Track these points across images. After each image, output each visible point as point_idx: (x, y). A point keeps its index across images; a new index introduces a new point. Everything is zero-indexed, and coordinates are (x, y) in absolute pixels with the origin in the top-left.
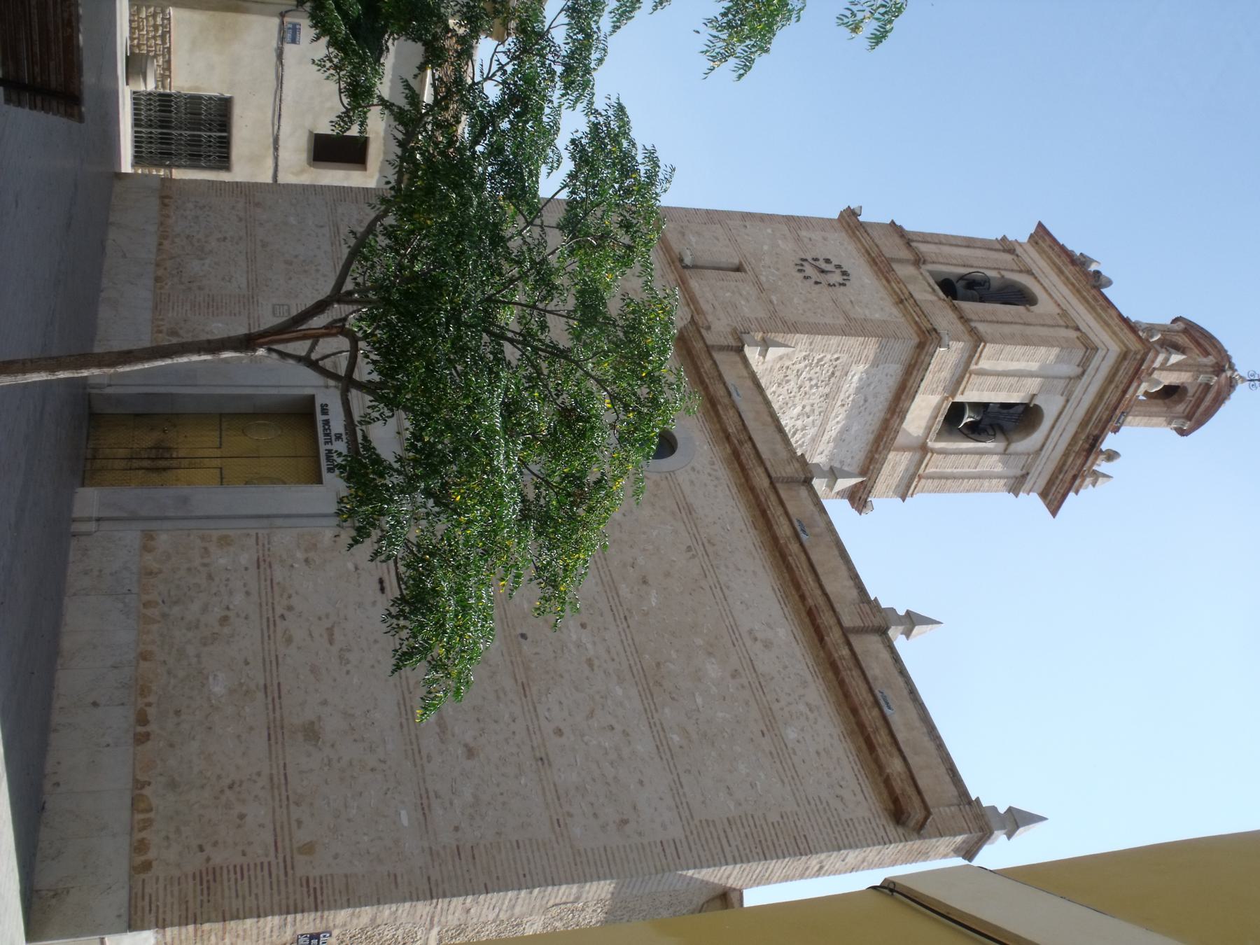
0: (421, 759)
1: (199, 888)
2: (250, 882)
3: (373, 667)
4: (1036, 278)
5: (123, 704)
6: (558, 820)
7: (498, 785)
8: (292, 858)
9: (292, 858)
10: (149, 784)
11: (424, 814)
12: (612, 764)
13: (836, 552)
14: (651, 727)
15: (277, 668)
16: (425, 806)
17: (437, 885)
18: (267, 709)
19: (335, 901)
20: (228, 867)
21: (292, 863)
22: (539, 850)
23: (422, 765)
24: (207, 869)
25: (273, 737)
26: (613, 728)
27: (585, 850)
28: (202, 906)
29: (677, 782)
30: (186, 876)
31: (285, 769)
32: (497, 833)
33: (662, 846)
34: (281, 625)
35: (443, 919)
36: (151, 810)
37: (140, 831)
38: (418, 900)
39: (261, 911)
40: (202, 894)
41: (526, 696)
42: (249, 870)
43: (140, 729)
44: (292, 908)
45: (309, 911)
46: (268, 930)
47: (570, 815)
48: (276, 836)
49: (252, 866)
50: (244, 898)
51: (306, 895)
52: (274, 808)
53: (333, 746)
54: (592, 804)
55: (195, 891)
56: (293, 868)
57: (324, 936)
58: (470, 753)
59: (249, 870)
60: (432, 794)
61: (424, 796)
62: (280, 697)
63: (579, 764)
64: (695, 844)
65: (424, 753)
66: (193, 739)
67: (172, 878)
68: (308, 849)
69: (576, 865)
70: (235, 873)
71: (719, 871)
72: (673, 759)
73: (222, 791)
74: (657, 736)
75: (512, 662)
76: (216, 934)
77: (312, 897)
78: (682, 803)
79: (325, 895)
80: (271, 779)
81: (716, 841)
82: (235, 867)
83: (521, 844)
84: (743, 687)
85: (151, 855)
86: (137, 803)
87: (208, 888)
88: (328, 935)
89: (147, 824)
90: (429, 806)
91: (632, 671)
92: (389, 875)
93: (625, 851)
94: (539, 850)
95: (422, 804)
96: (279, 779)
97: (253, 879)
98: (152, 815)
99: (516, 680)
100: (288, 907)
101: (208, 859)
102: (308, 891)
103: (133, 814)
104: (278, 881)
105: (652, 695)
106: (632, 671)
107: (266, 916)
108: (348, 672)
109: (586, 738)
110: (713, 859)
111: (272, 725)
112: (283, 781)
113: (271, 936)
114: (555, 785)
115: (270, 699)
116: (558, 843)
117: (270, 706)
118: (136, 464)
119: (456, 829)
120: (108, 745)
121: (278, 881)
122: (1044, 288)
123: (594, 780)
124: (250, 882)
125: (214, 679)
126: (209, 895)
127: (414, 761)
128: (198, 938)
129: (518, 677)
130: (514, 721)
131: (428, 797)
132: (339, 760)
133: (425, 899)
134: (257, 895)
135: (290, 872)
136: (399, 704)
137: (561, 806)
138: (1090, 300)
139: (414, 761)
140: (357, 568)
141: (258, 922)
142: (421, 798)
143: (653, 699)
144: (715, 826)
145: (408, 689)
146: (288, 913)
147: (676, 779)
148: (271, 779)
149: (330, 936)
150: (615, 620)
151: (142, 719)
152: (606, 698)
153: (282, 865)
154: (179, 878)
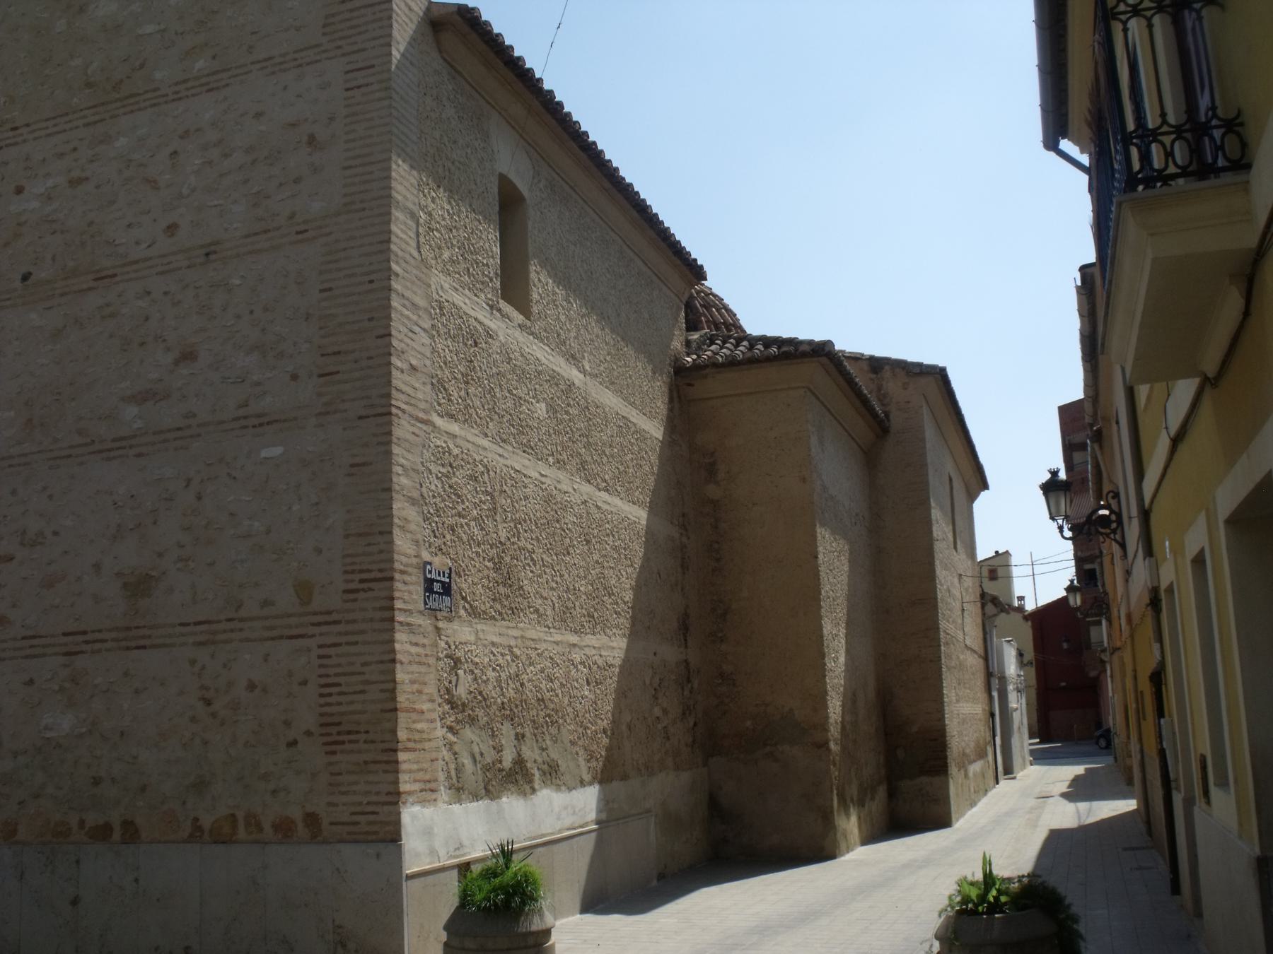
0: (189, 427)
1: (347, 746)
2: (344, 674)
3: (50, 497)
5: (78, 862)
6: (298, 233)
7: (239, 317)
8: (315, 614)
9: (315, 614)
10: (196, 820)
11: (268, 423)
12: (226, 156)
14: (180, 99)
15: (41, 637)
16: (256, 421)
17: (372, 406)
18: (99, 651)
19: (381, 552)
20: (321, 706)
21: (321, 613)
22: (336, 261)
23: (199, 426)
24: (322, 735)
25: (142, 642)
26: (175, 152)
27: (345, 195)
28: (373, 742)
29: (264, 64)
30: (330, 764)
31: (188, 624)
32: (307, 319)
33: (352, 89)
35: (422, 405)
36: (233, 815)
37: (261, 830)
38: (390, 433)
39: (386, 657)
40: (357, 742)
41: (115, 275)
42: (328, 676)
43: (117, 835)
44: (387, 614)
45: (392, 589)
46: (414, 650)
47: (292, 217)
48: (281, 637)
49: (323, 671)
50: (367, 682)
51: (370, 594)
52: (241, 641)
54: (281, 185)
55: (352, 751)
56: (329, 613)
57: (430, 572)
58: (188, 356)
59: (328, 676)
60: (241, 412)
61: (243, 422)
62: (85, 633)
63: (221, 202)
64: (356, 43)
66: (135, 758)
67: (330, 784)
68: (304, 591)
69: (364, 209)
70: (330, 695)
71: (397, 15)
72: (229, 70)
73: (214, 715)
74: (193, 91)
75: (62, 295)
76: (414, 722)
77: (371, 585)
78: (296, 59)
79: (370, 567)
80: (201, 644)
81: (355, 14)
82: (322, 695)
83: (326, 285)
85: (296, 813)
86: (222, 836)
87: (349, 733)
88: (428, 567)
89: (253, 822)
90: (259, 416)
91: (95, 123)
92: (350, 475)
93: (354, 140)
94: (336, 261)
95: (254, 427)
96: (201, 633)
97: (340, 670)
98: (240, 815)
99: (90, 289)
100: (383, 620)
101: (309, 733)
102: (363, 590)
103: (235, 842)
104: (346, 633)
105: (132, 96)
106: (95, 123)
107: (393, 651)
108: (56, 533)
109: (185, 191)
110: (381, 19)
111: (124, 644)
113: (424, 646)
114: (247, 236)
115: (84, 647)
116: (331, 233)
117: (97, 646)
119: (294, 377)
120: (136, 880)
121: (346, 633)
123: (246, 182)
124: (344, 674)
125: (51, 729)
126: (357, 732)
127: (192, 436)
128: (419, 746)
129: (85, 286)
130: (149, 293)
131: (245, 418)
133: (390, 423)
134: (364, 664)
135: (335, 617)
136: (109, 459)
137: (278, 228)
139: (192, 436)
141: (402, 663)
142: (245, 427)
143: (139, 94)
144: (333, 15)
145: (86, 445)
146: (392, 619)
147: (258, 66)
148: (201, 644)
149: (430, 564)
150: (16, 144)
151: (103, 833)
152: (130, 161)
153: (324, 629)
154: (332, 774)
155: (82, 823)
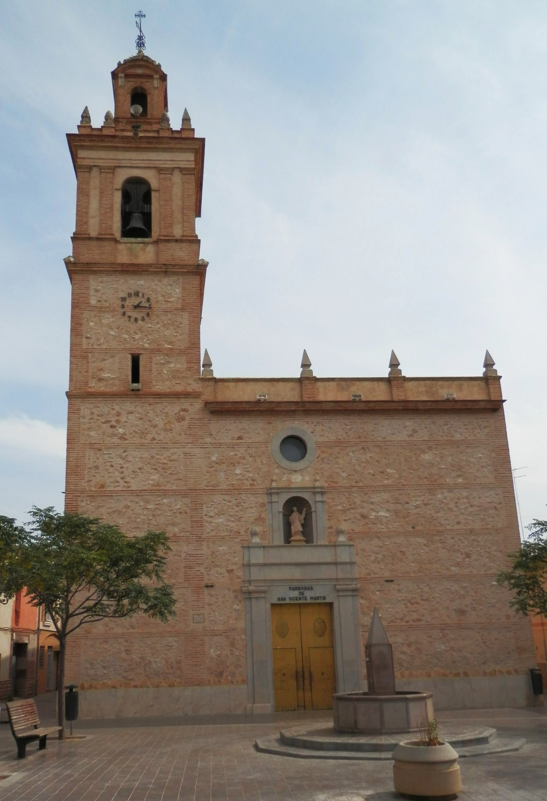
4: (119, 167)
13: (358, 383)
34: (411, 623)
53: (467, 606)
58: (468, 556)
60: (486, 573)
65: (469, 573)
73: (487, 646)
84: (436, 448)
86: (493, 673)
101: (513, 650)
108: (433, 598)
112: (482, 624)
118: (307, 686)
122: (130, 167)
132: (472, 604)
136: (448, 580)
138: (148, 146)
140: (379, 591)
151: (458, 675)
155: (451, 673)
